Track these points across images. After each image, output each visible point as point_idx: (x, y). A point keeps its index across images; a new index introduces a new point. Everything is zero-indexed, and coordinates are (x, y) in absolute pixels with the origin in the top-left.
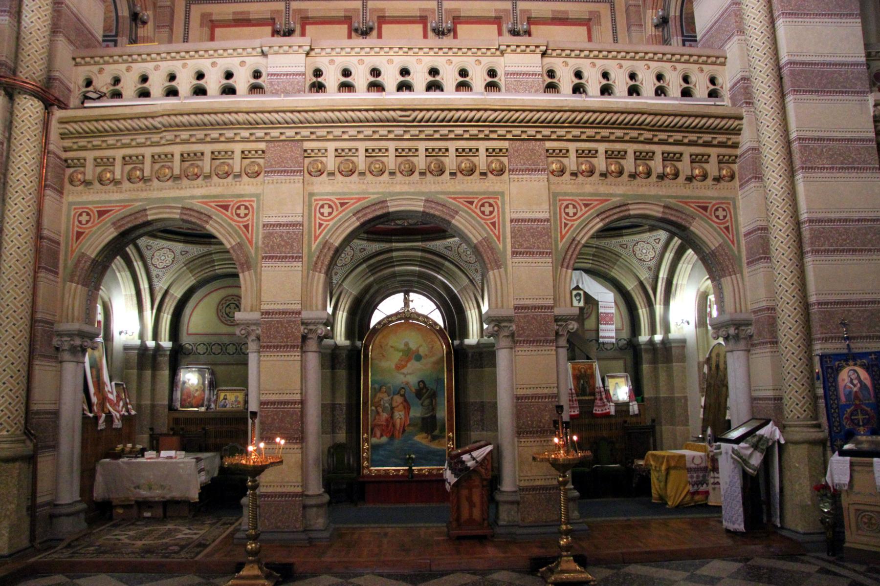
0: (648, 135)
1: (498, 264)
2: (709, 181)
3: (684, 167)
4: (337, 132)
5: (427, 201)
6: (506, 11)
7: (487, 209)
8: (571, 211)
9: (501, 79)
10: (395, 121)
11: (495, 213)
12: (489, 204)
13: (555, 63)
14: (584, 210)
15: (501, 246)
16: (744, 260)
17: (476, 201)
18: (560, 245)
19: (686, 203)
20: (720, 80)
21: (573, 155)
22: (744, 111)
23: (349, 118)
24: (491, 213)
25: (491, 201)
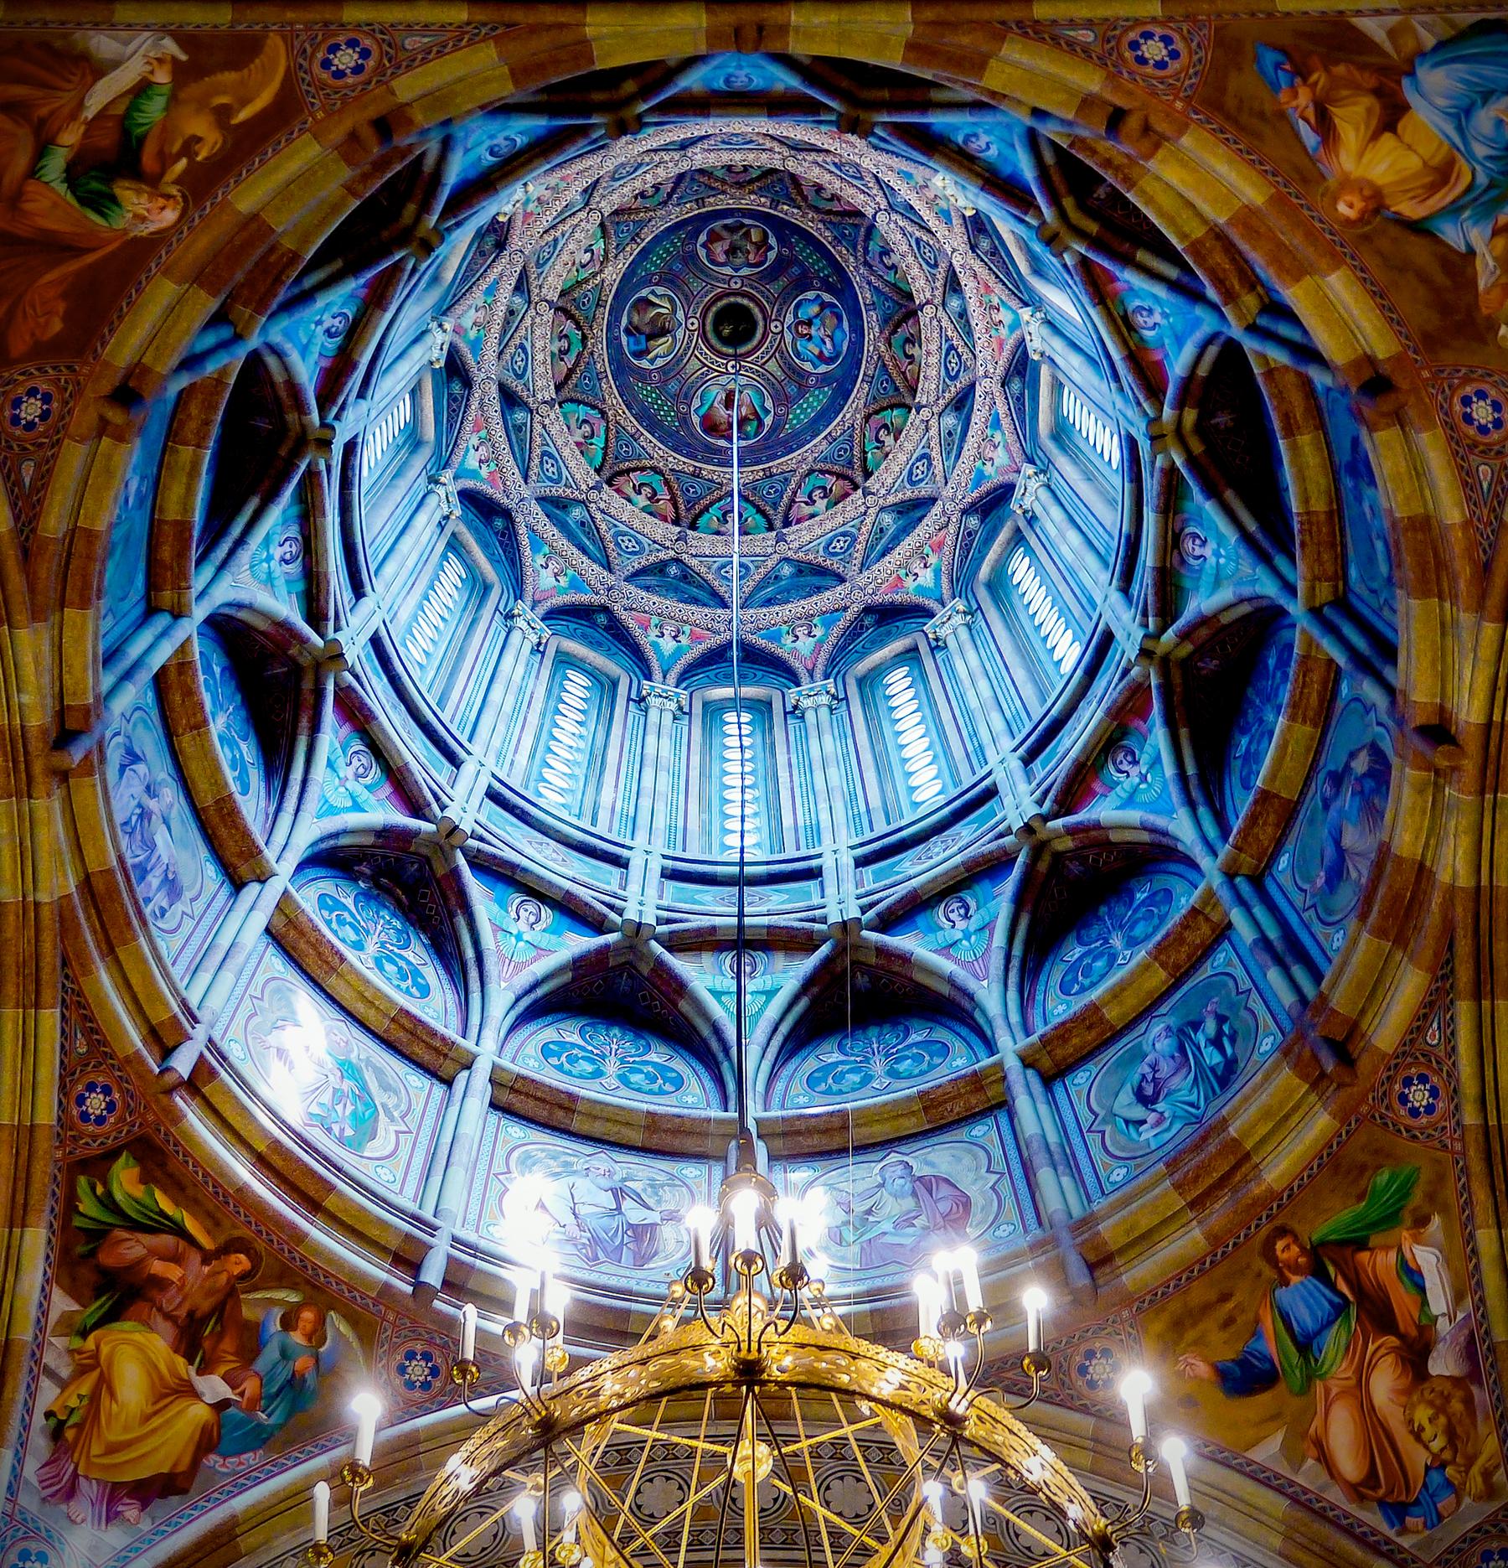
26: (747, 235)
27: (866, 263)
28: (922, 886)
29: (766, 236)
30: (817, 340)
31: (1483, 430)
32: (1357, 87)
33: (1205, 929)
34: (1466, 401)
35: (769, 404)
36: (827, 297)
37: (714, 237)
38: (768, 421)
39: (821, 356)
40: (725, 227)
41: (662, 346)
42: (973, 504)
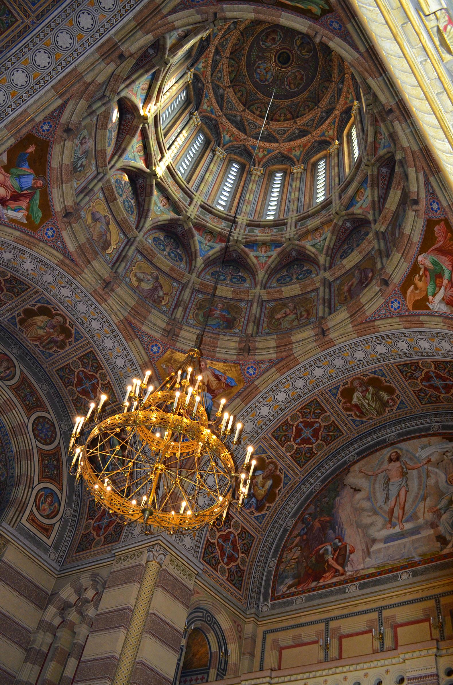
26: (294, 85)
27: (263, 103)
28: (157, 84)
29: (290, 88)
30: (262, 70)
31: (153, 346)
32: (218, 389)
33: (100, 165)
34: (159, 348)
35: (263, 46)
36: (267, 83)
37: (302, 79)
38: (261, 43)
39: (258, 67)
40: (301, 84)
41: (299, 42)
42: (203, 89)
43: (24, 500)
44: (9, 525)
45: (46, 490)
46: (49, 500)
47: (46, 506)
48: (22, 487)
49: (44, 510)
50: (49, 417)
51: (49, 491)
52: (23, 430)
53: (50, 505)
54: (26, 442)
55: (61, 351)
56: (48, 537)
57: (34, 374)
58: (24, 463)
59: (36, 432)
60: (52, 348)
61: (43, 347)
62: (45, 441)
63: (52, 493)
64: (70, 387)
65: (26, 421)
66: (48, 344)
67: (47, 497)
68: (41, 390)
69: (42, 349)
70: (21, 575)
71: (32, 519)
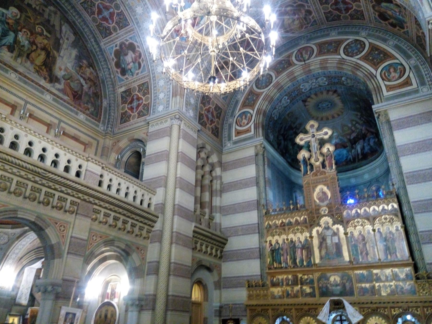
0: (129, 214)
1: (60, 256)
2: (142, 238)
3: (136, 230)
4: (7, 167)
5: (37, 217)
6: (55, 124)
7: (62, 228)
8: (95, 238)
9: (83, 170)
10: (39, 173)
11: (65, 232)
12: (63, 226)
13: (105, 173)
14: (99, 239)
15: (63, 248)
16: (146, 273)
17: (58, 223)
18: (87, 253)
19: (133, 245)
20: (152, 200)
21: (102, 214)
22: (160, 215)
23: (18, 163)
24: (64, 231)
25: (65, 225)
43: (375, 86)
44: (378, 103)
45: (385, 69)
46: (392, 70)
47: (393, 74)
48: (368, 83)
49: (393, 77)
50: (351, 40)
51: (387, 67)
52: (342, 62)
53: (395, 71)
54: (349, 64)
55: (313, 14)
56: (411, 85)
57: (323, 36)
58: (359, 73)
59: (350, 54)
60: (310, 19)
61: (308, 24)
62: (359, 51)
63: (390, 65)
64: (341, 18)
65: (339, 57)
66: (306, 20)
67: (389, 70)
68: (334, 36)
69: (309, 25)
70: (411, 116)
71: (389, 88)
